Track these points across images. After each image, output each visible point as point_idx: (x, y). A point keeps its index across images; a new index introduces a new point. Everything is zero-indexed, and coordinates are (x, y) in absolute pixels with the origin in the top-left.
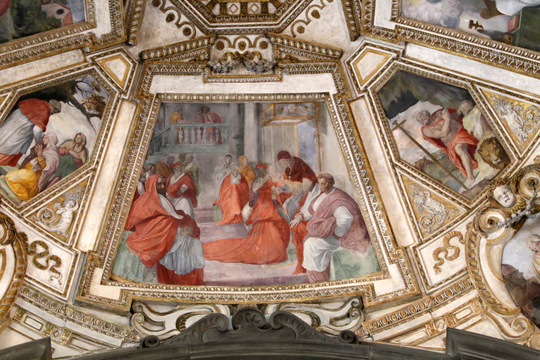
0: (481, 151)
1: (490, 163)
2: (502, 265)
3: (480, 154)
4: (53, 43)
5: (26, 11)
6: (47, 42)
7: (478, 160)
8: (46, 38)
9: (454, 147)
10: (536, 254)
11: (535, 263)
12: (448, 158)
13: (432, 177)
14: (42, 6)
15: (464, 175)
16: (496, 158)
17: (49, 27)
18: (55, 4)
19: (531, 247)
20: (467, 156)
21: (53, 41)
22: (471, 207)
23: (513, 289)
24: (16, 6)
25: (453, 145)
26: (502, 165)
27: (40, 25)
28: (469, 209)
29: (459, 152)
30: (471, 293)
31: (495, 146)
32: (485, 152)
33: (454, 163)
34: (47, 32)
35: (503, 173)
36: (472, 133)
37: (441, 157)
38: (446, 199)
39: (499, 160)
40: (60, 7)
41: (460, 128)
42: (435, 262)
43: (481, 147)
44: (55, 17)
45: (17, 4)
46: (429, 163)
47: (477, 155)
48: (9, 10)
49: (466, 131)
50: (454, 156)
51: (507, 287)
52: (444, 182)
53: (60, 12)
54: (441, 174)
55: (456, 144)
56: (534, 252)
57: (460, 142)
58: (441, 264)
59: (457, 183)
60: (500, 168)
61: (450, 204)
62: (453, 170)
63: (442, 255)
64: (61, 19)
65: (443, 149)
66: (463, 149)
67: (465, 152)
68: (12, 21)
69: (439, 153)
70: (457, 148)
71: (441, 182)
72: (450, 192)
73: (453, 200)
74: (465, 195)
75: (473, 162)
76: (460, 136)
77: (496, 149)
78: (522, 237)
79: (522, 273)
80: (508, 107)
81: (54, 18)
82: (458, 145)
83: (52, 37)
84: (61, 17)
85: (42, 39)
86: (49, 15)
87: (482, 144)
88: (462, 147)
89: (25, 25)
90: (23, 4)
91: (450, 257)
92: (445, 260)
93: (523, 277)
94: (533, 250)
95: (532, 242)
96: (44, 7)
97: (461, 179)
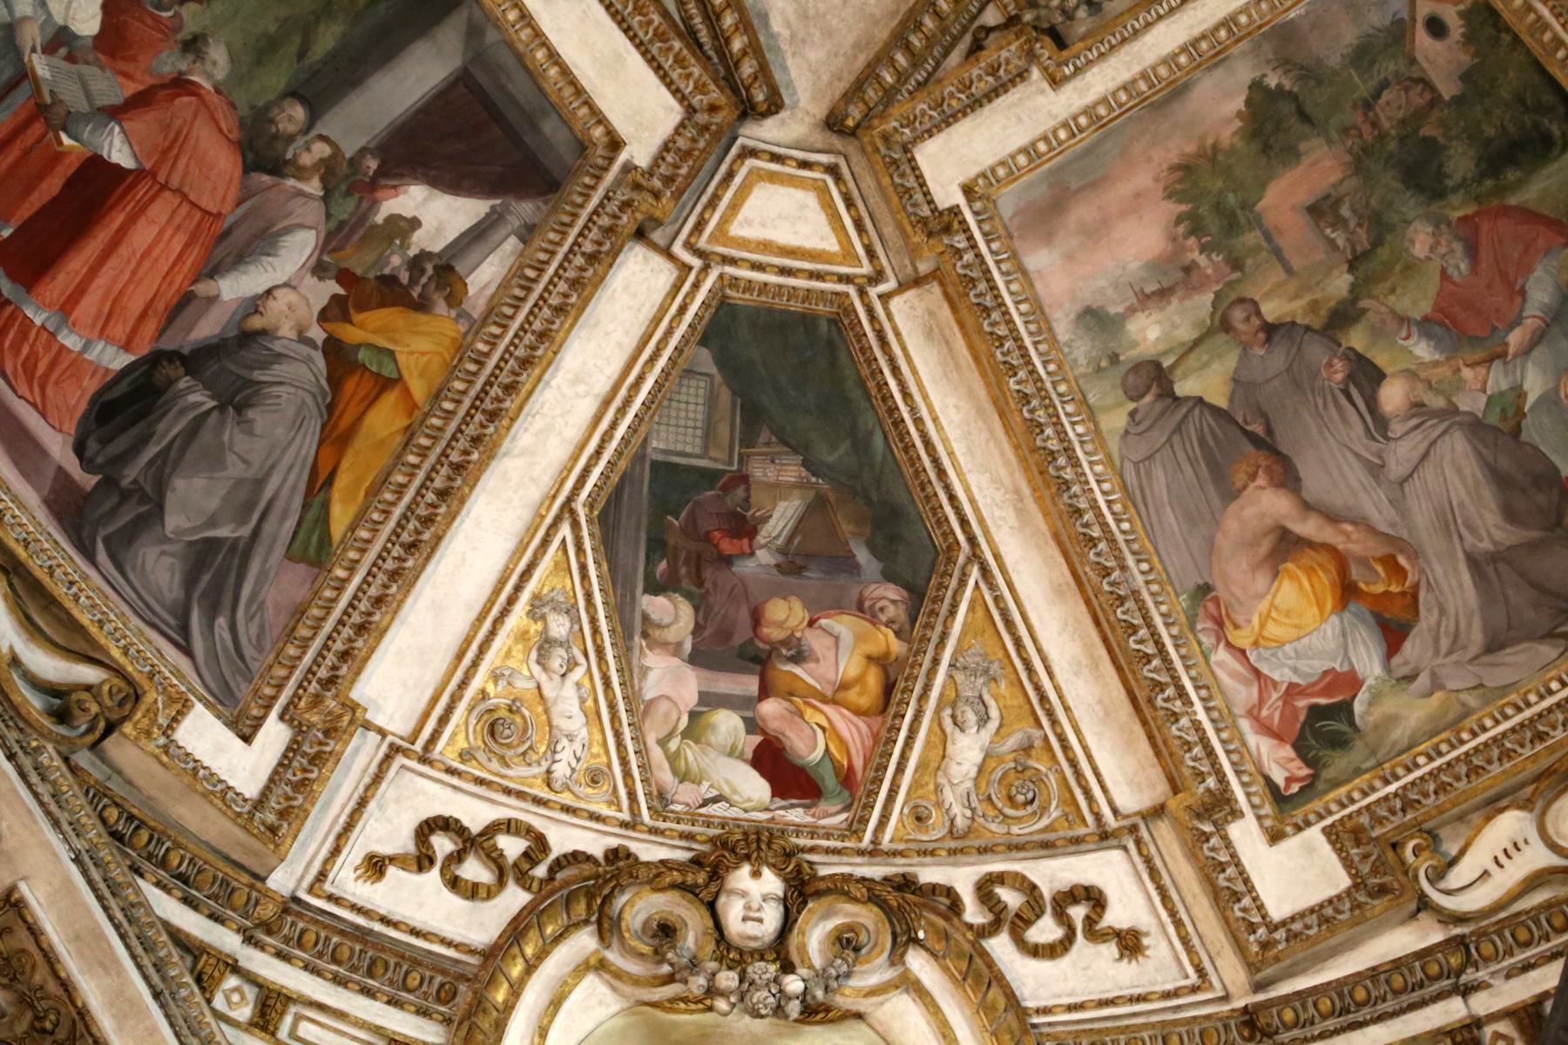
4: (1552, 9)
5: (1488, 141)
6: (1558, 28)
8: (1547, 37)
14: (1447, 97)
17: (1506, 38)
18: (1420, 58)
21: (1545, 12)
24: (1489, 183)
27: (1512, 74)
34: (1526, 38)
40: (1422, 38)
44: (1463, 35)
45: (1480, 183)
48: (1513, 201)
53: (1436, 27)
64: (1461, 15)
68: (1545, 172)
81: (1469, 38)
83: (1532, 16)
84: (1450, 15)
85: (1557, 49)
86: (1466, 59)
89: (1536, 125)
90: (1472, 165)
96: (1448, 89)
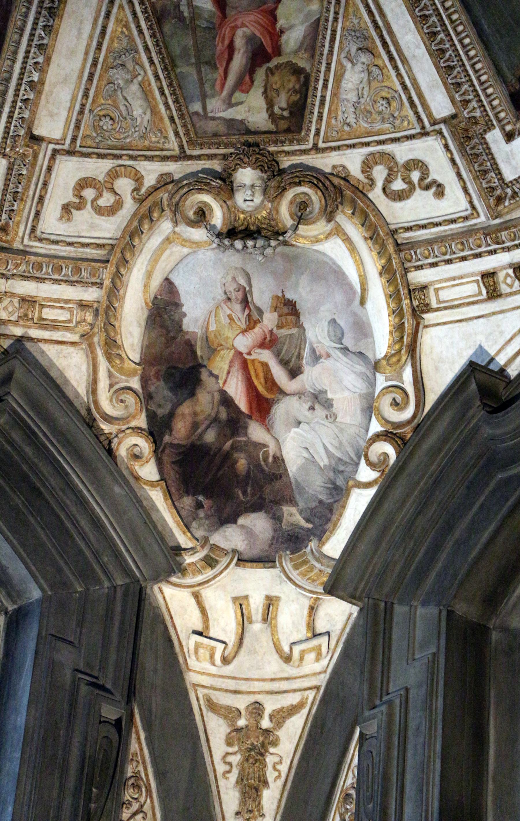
0: (273, 74)
1: (270, 105)
2: (167, 279)
3: (267, 76)
7: (256, 83)
9: (236, 27)
10: (225, 303)
11: (213, 313)
12: (214, 38)
13: (166, 48)
15: (218, 87)
16: (284, 105)
19: (227, 285)
20: (244, 61)
22: (188, 152)
23: (154, 328)
25: (239, 23)
26: (283, 125)
28: (184, 152)
29: (239, 42)
30: (90, 290)
31: (297, 87)
32: (276, 80)
33: (217, 53)
35: (275, 142)
36: (282, 32)
37: (204, 25)
38: (162, 108)
39: (286, 114)
41: (270, 5)
42: (69, 197)
43: (277, 67)
46: (181, 19)
47: (260, 74)
49: (274, 19)
50: (226, 42)
51: (149, 318)
52: (178, 70)
54: (185, 49)
55: (243, 25)
56: (224, 297)
57: (252, 28)
58: (80, 207)
59: (197, 92)
60: (277, 126)
61: (161, 119)
62: (206, 63)
63: (89, 193)
65: (218, 13)
66: (247, 43)
67: (246, 51)
69: (206, 15)
70: (240, 33)
71: (174, 66)
72: (176, 101)
73: (172, 119)
74: (195, 118)
75: (247, 78)
76: (260, 18)
77: (295, 92)
78: (225, 260)
79: (185, 315)
80: (364, 58)
82: (245, 29)
87: (282, 65)
88: (250, 39)
91: (100, 207)
92: (89, 206)
93: (181, 321)
94: (225, 293)
95: (234, 279)
97: (207, 87)
